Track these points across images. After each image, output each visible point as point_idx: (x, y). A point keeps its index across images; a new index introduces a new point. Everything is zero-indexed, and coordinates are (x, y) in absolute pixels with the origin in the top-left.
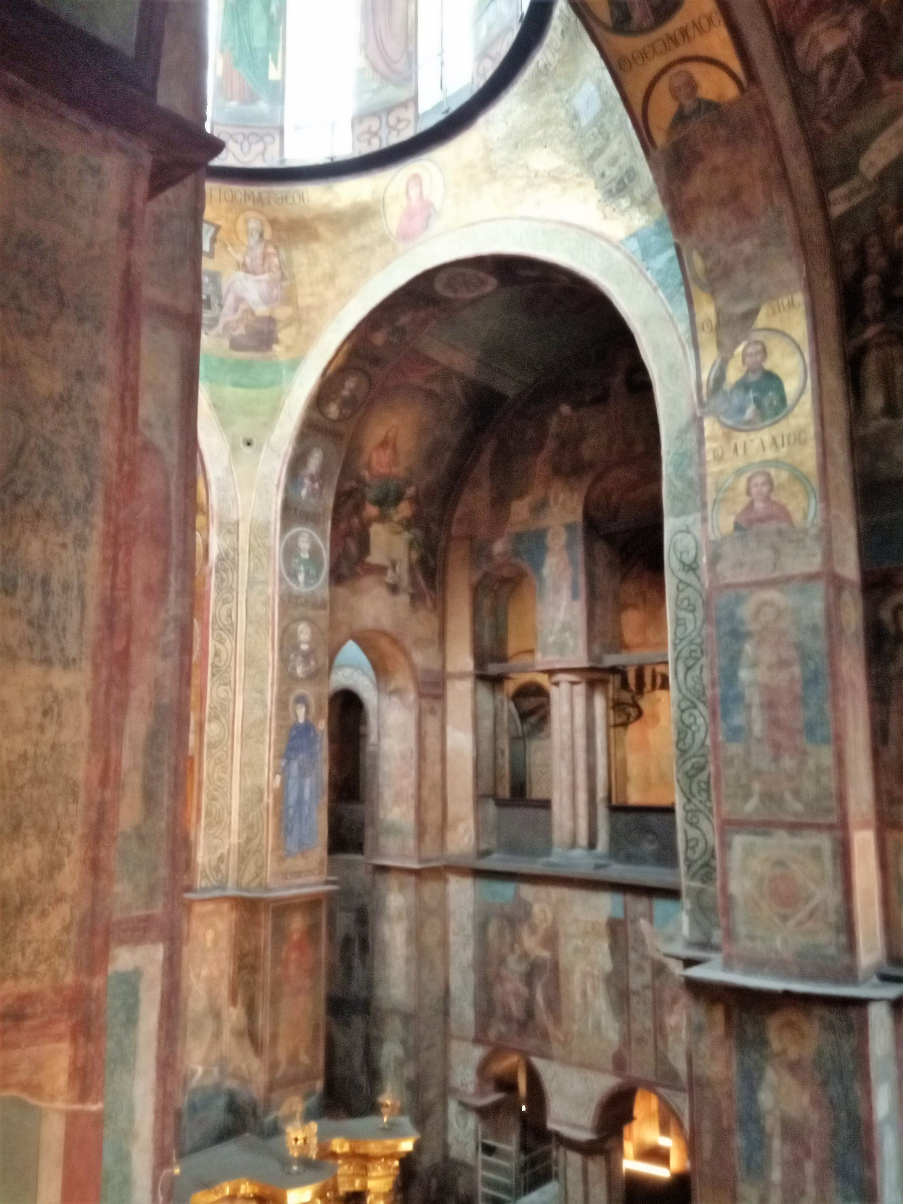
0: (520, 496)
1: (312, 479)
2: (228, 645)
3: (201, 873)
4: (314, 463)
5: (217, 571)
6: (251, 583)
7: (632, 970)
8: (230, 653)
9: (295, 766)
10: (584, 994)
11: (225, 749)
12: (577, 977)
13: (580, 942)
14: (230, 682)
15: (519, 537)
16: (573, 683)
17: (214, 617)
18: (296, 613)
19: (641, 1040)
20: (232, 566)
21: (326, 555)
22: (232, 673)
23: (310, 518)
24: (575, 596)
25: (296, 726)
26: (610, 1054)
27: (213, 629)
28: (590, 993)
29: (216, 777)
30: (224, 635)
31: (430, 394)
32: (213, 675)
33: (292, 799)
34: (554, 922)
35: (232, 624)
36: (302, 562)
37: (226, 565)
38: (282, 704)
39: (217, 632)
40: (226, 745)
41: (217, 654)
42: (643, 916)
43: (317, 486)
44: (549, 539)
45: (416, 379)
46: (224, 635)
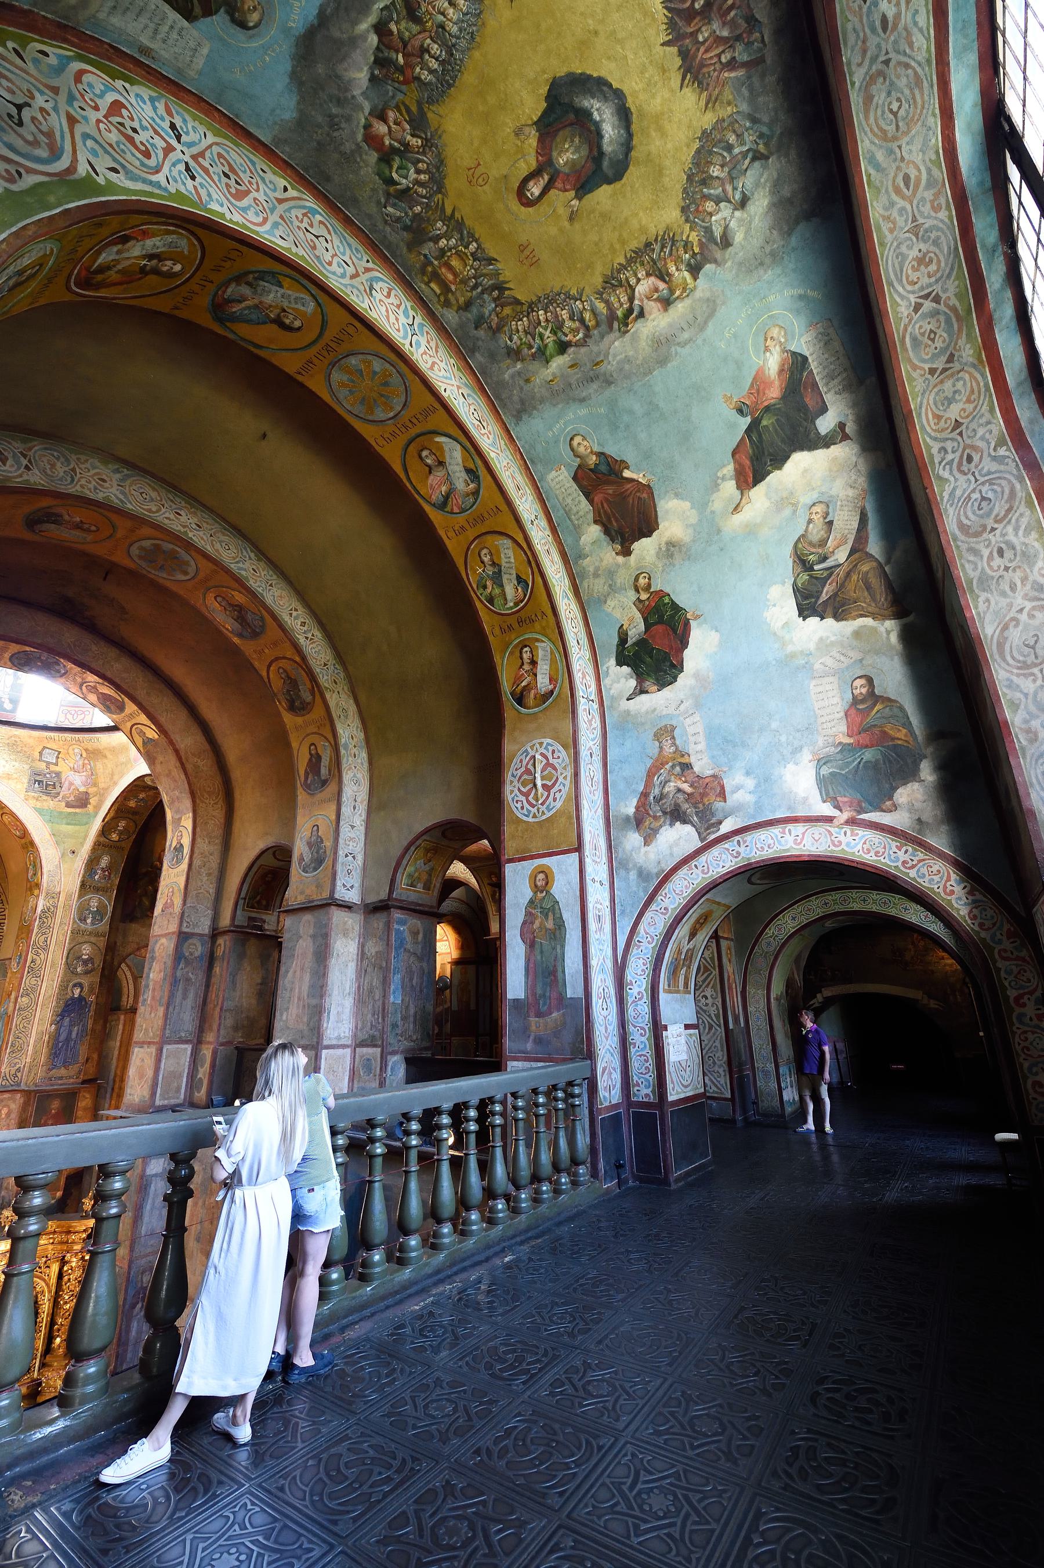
2: (42, 956)
4: (105, 861)
9: (67, 1020)
17: (35, 942)
18: (81, 940)
21: (110, 909)
23: (97, 890)
25: (72, 999)
33: (62, 1038)
36: (91, 912)
38: (63, 987)
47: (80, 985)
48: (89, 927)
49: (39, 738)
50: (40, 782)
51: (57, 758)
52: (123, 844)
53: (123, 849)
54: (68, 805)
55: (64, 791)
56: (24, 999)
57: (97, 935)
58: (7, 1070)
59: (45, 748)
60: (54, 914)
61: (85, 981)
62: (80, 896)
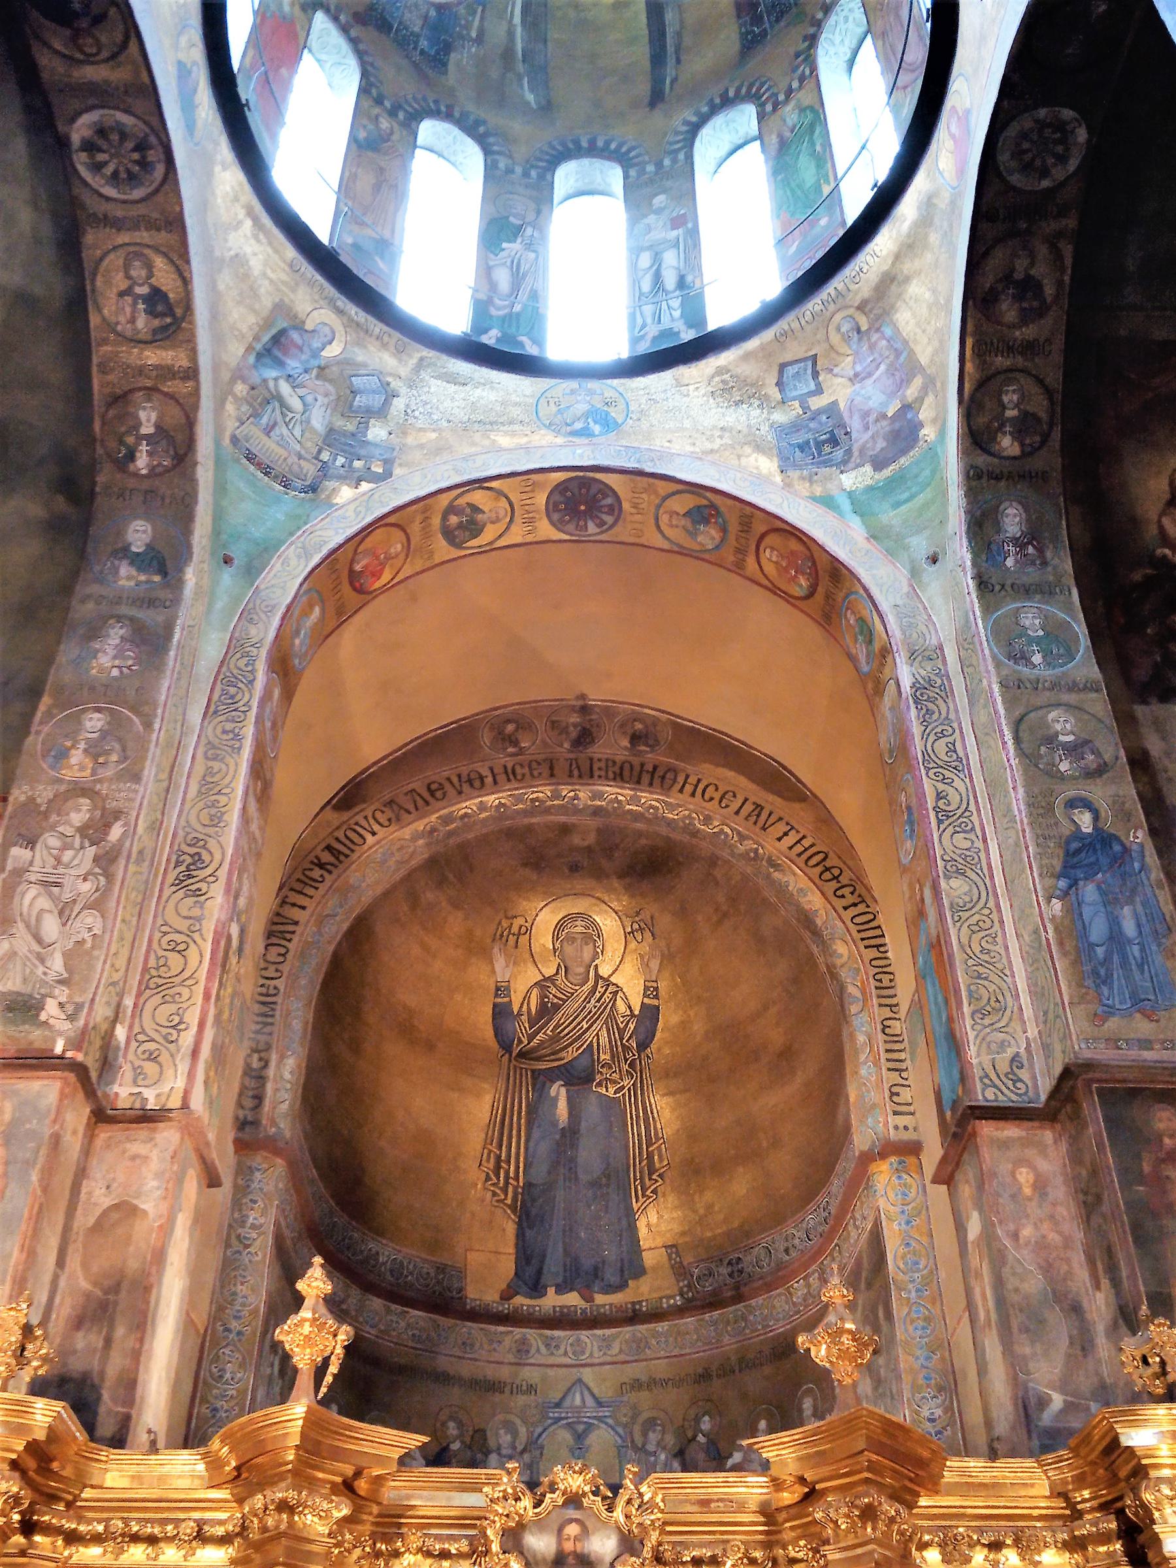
2: (958, 783)
3: (981, 1079)
5: (915, 702)
8: (964, 796)
11: (986, 912)
14: (973, 829)
20: (943, 694)
22: (975, 818)
27: (928, 769)
29: (977, 950)
30: (947, 774)
32: (940, 822)
35: (959, 759)
37: (931, 694)
38: (1040, 807)
39: (932, 771)
40: (985, 907)
41: (939, 796)
43: (1031, 550)
46: (947, 774)
47: (1087, 805)
48: (1048, 673)
49: (765, 353)
50: (803, 447)
51: (815, 375)
52: (1037, 463)
53: (1044, 476)
54: (878, 465)
55: (860, 437)
56: (954, 883)
57: (1073, 687)
58: (986, 1060)
59: (782, 367)
60: (946, 693)
61: (1099, 793)
62: (987, 610)
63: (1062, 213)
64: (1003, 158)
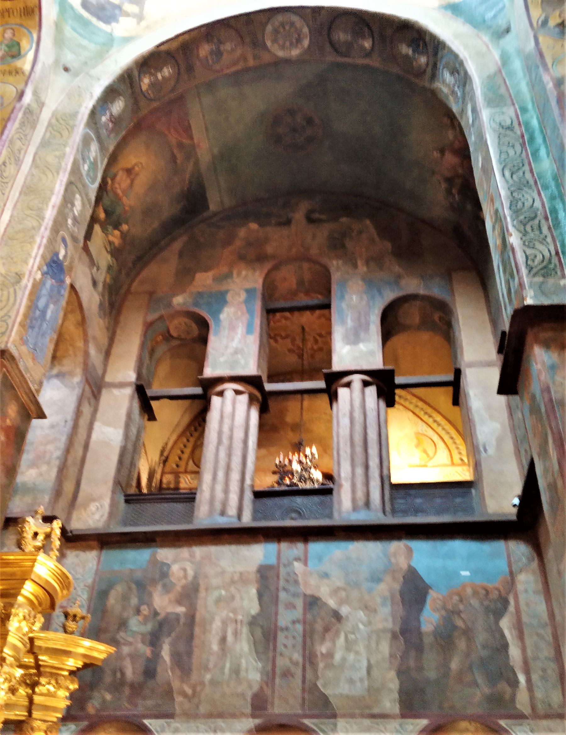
0: (207, 269)
1: (111, 115)
6: (44, 144)
7: (281, 609)
10: (223, 640)
12: (217, 625)
13: (223, 592)
15: (200, 295)
16: (238, 392)
19: (287, 674)
24: (249, 330)
26: (249, 694)
28: (230, 638)
31: (174, 158)
34: (195, 577)
42: (297, 559)
44: (229, 297)
45: (173, 138)
63: (255, 57)
64: (280, 18)
